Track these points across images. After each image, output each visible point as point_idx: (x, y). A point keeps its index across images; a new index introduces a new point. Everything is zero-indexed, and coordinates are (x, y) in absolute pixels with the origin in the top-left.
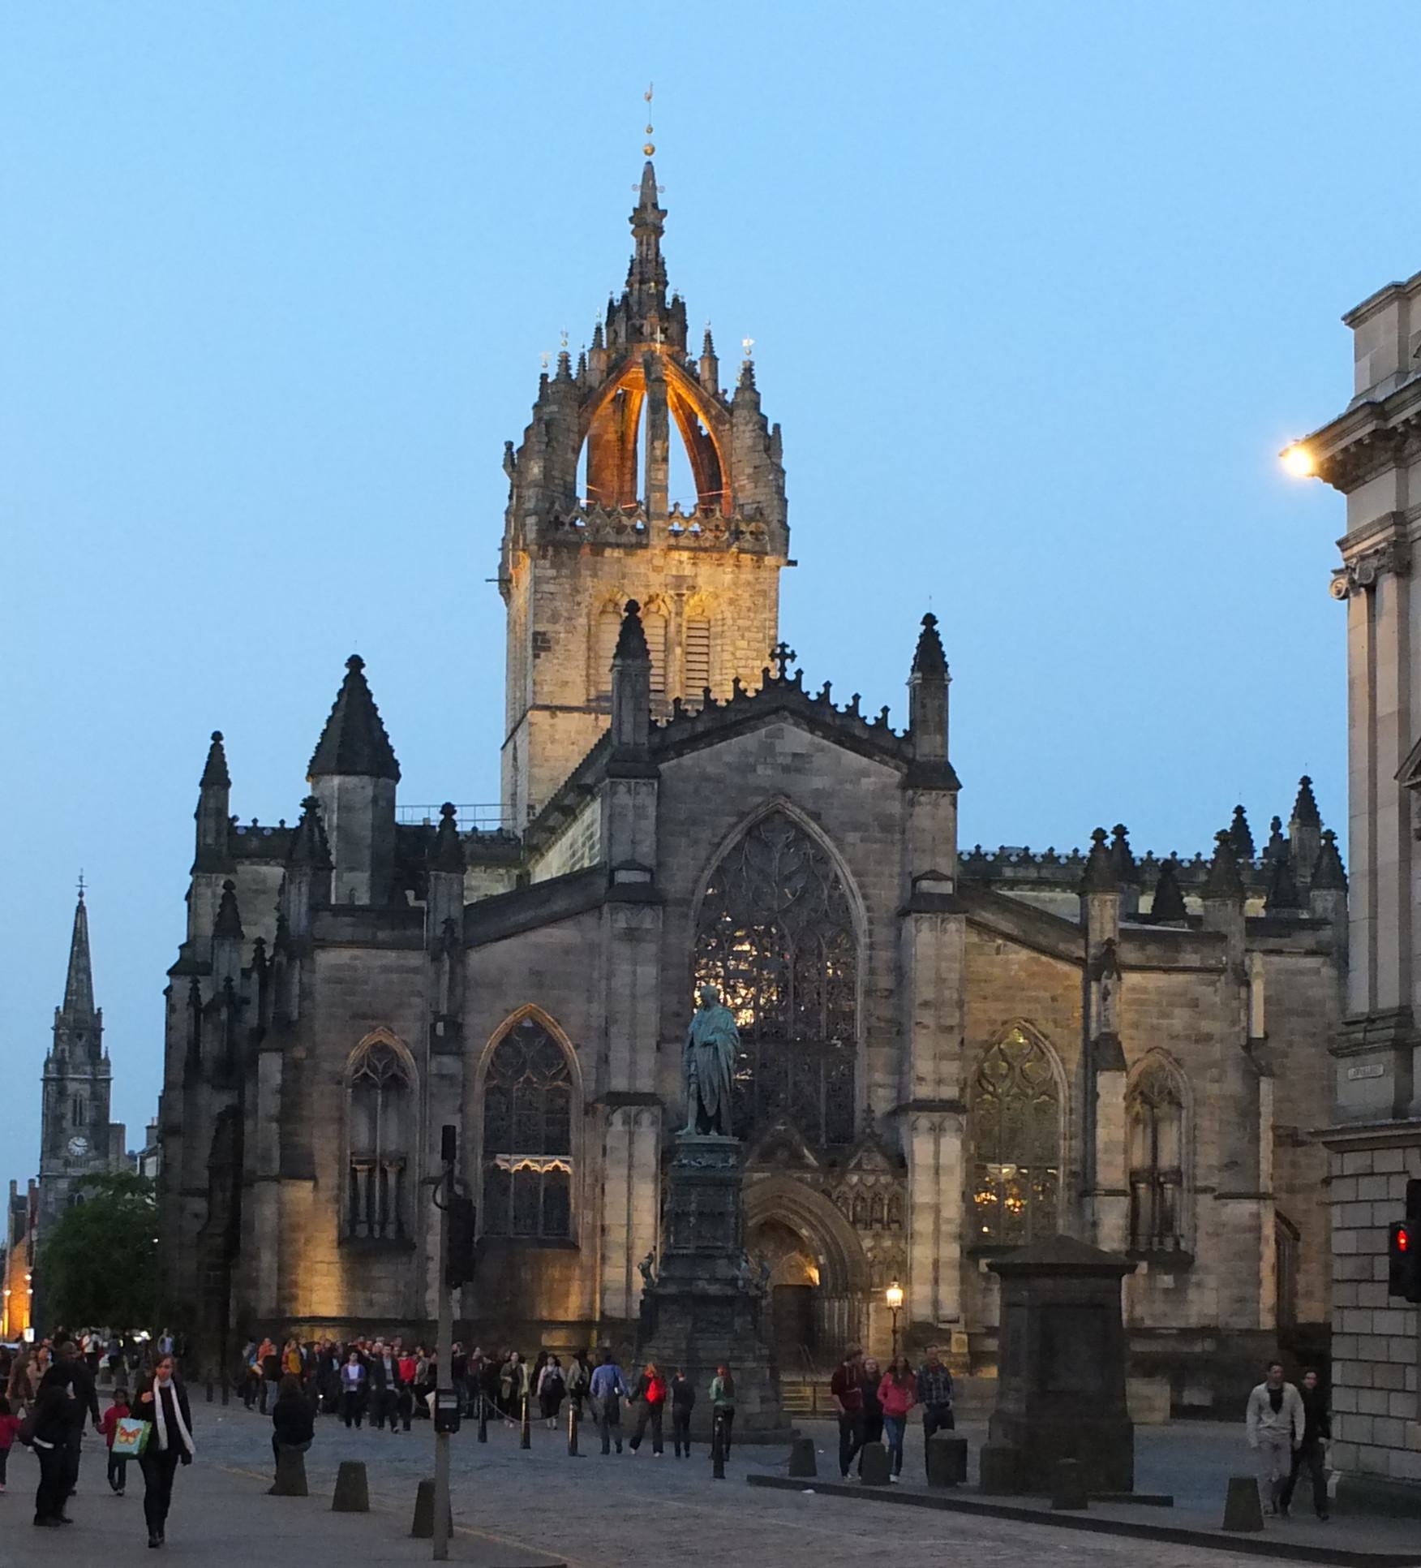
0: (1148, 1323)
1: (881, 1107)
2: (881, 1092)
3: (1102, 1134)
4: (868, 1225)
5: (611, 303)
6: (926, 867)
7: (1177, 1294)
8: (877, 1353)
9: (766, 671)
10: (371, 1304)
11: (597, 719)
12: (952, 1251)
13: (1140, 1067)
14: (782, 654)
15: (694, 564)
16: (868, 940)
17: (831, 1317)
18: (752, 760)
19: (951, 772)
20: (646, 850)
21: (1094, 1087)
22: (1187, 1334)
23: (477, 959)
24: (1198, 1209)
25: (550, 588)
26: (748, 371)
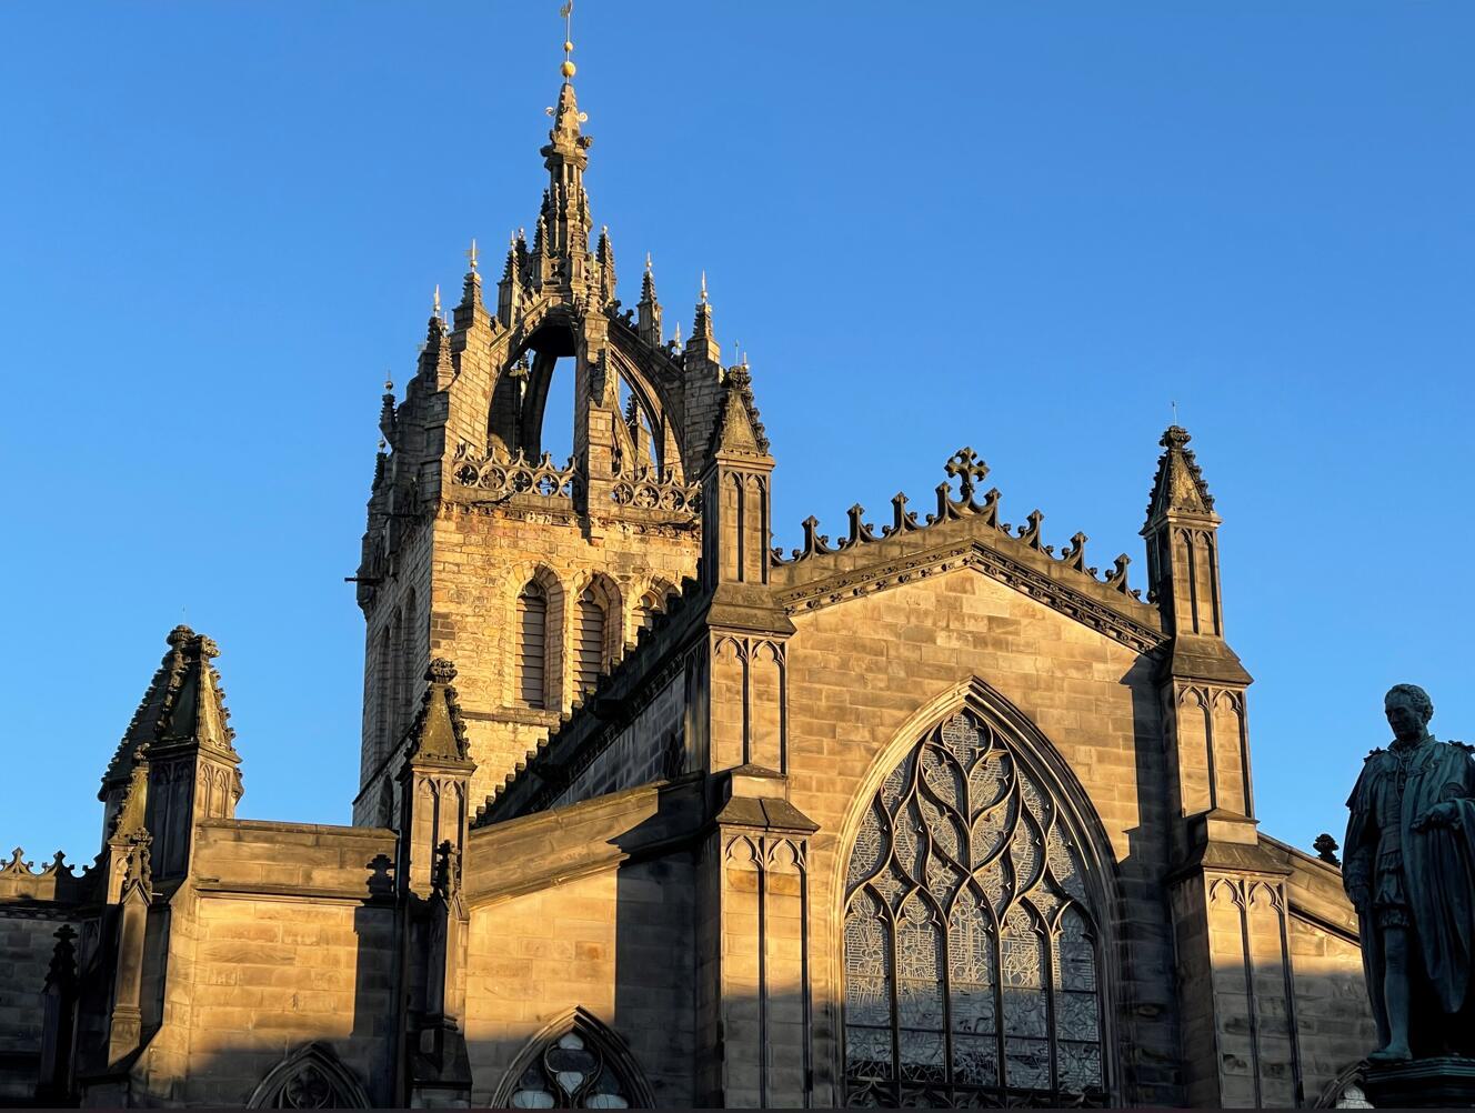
5: (521, 246)
9: (940, 492)
11: (515, 731)
14: (966, 467)
15: (642, 540)
16: (1118, 922)
18: (929, 623)
19: (1230, 660)
25: (458, 558)
26: (701, 318)
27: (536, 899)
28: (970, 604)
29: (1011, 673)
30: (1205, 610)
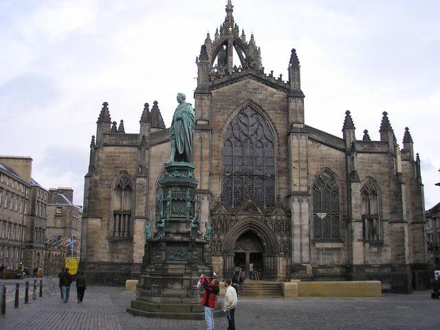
0: (370, 263)
1: (283, 194)
2: (283, 190)
3: (353, 202)
4: (279, 231)
6: (294, 120)
7: (378, 254)
8: (283, 274)
10: (118, 257)
12: (306, 240)
13: (365, 181)
17: (268, 263)
19: (302, 92)
20: (206, 116)
21: (350, 186)
22: (383, 266)
23: (154, 149)
24: (384, 227)
26: (252, 37)
27: (163, 145)
28: (249, 86)
29: (257, 98)
30: (297, 83)
